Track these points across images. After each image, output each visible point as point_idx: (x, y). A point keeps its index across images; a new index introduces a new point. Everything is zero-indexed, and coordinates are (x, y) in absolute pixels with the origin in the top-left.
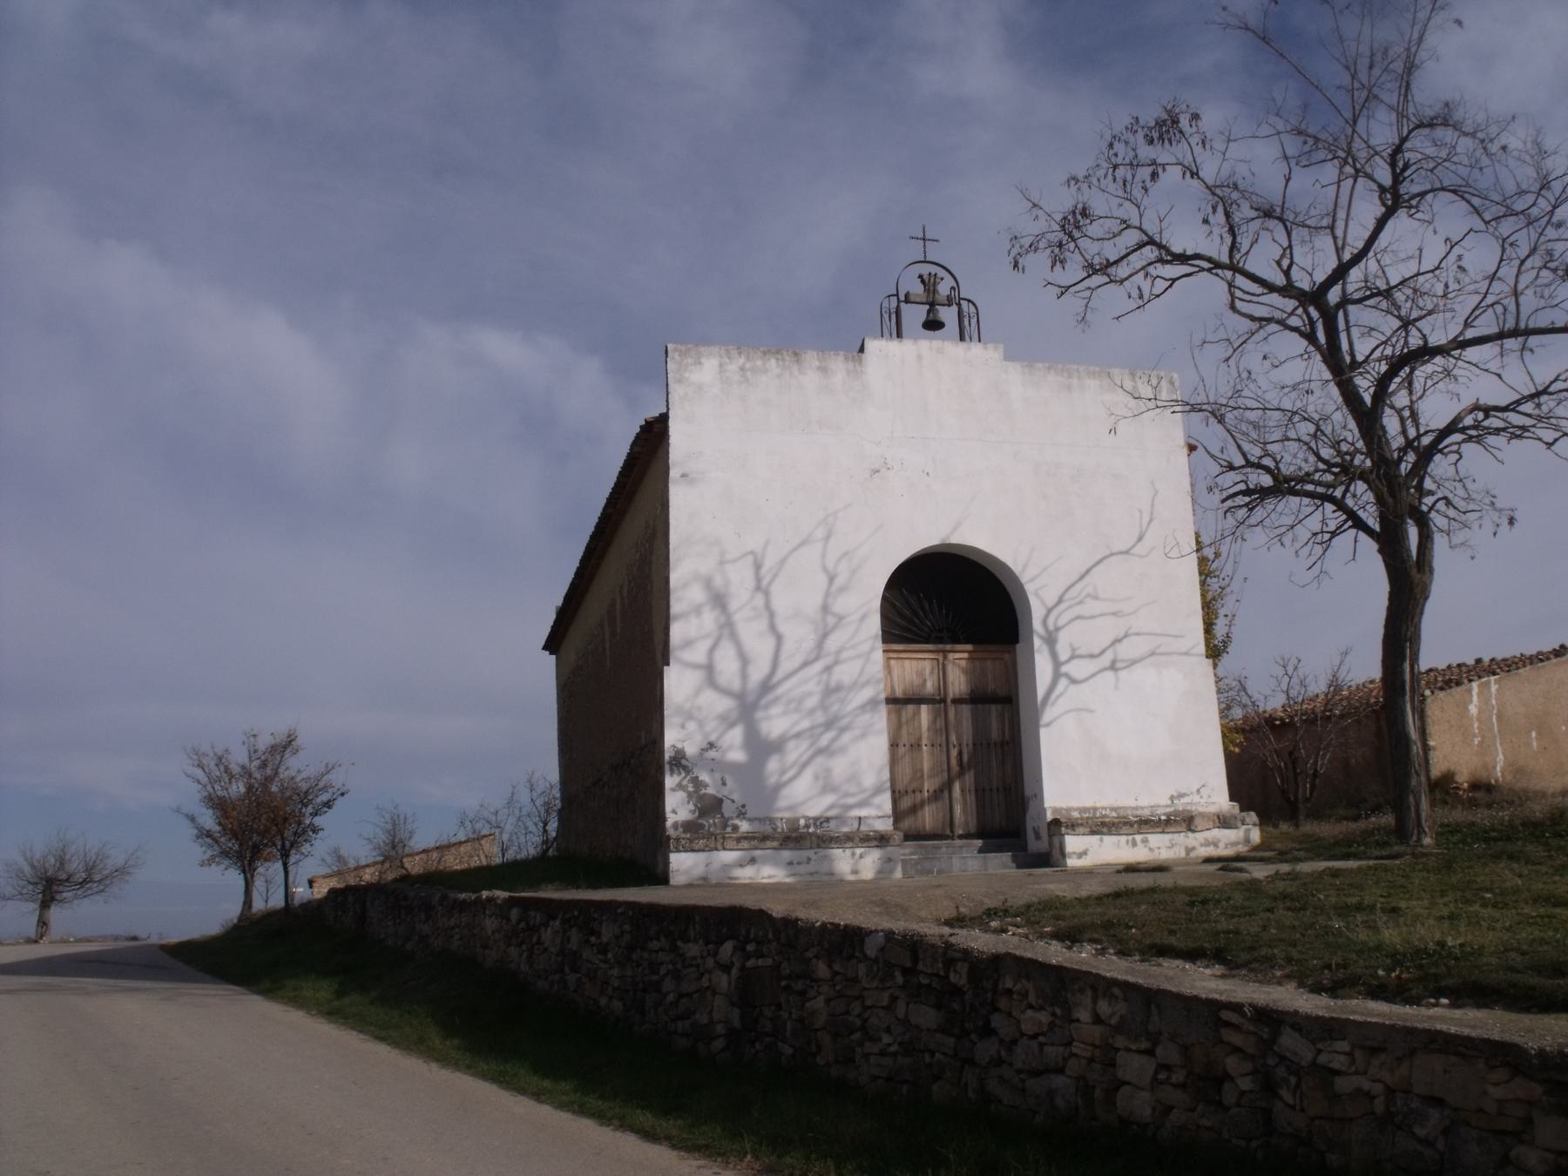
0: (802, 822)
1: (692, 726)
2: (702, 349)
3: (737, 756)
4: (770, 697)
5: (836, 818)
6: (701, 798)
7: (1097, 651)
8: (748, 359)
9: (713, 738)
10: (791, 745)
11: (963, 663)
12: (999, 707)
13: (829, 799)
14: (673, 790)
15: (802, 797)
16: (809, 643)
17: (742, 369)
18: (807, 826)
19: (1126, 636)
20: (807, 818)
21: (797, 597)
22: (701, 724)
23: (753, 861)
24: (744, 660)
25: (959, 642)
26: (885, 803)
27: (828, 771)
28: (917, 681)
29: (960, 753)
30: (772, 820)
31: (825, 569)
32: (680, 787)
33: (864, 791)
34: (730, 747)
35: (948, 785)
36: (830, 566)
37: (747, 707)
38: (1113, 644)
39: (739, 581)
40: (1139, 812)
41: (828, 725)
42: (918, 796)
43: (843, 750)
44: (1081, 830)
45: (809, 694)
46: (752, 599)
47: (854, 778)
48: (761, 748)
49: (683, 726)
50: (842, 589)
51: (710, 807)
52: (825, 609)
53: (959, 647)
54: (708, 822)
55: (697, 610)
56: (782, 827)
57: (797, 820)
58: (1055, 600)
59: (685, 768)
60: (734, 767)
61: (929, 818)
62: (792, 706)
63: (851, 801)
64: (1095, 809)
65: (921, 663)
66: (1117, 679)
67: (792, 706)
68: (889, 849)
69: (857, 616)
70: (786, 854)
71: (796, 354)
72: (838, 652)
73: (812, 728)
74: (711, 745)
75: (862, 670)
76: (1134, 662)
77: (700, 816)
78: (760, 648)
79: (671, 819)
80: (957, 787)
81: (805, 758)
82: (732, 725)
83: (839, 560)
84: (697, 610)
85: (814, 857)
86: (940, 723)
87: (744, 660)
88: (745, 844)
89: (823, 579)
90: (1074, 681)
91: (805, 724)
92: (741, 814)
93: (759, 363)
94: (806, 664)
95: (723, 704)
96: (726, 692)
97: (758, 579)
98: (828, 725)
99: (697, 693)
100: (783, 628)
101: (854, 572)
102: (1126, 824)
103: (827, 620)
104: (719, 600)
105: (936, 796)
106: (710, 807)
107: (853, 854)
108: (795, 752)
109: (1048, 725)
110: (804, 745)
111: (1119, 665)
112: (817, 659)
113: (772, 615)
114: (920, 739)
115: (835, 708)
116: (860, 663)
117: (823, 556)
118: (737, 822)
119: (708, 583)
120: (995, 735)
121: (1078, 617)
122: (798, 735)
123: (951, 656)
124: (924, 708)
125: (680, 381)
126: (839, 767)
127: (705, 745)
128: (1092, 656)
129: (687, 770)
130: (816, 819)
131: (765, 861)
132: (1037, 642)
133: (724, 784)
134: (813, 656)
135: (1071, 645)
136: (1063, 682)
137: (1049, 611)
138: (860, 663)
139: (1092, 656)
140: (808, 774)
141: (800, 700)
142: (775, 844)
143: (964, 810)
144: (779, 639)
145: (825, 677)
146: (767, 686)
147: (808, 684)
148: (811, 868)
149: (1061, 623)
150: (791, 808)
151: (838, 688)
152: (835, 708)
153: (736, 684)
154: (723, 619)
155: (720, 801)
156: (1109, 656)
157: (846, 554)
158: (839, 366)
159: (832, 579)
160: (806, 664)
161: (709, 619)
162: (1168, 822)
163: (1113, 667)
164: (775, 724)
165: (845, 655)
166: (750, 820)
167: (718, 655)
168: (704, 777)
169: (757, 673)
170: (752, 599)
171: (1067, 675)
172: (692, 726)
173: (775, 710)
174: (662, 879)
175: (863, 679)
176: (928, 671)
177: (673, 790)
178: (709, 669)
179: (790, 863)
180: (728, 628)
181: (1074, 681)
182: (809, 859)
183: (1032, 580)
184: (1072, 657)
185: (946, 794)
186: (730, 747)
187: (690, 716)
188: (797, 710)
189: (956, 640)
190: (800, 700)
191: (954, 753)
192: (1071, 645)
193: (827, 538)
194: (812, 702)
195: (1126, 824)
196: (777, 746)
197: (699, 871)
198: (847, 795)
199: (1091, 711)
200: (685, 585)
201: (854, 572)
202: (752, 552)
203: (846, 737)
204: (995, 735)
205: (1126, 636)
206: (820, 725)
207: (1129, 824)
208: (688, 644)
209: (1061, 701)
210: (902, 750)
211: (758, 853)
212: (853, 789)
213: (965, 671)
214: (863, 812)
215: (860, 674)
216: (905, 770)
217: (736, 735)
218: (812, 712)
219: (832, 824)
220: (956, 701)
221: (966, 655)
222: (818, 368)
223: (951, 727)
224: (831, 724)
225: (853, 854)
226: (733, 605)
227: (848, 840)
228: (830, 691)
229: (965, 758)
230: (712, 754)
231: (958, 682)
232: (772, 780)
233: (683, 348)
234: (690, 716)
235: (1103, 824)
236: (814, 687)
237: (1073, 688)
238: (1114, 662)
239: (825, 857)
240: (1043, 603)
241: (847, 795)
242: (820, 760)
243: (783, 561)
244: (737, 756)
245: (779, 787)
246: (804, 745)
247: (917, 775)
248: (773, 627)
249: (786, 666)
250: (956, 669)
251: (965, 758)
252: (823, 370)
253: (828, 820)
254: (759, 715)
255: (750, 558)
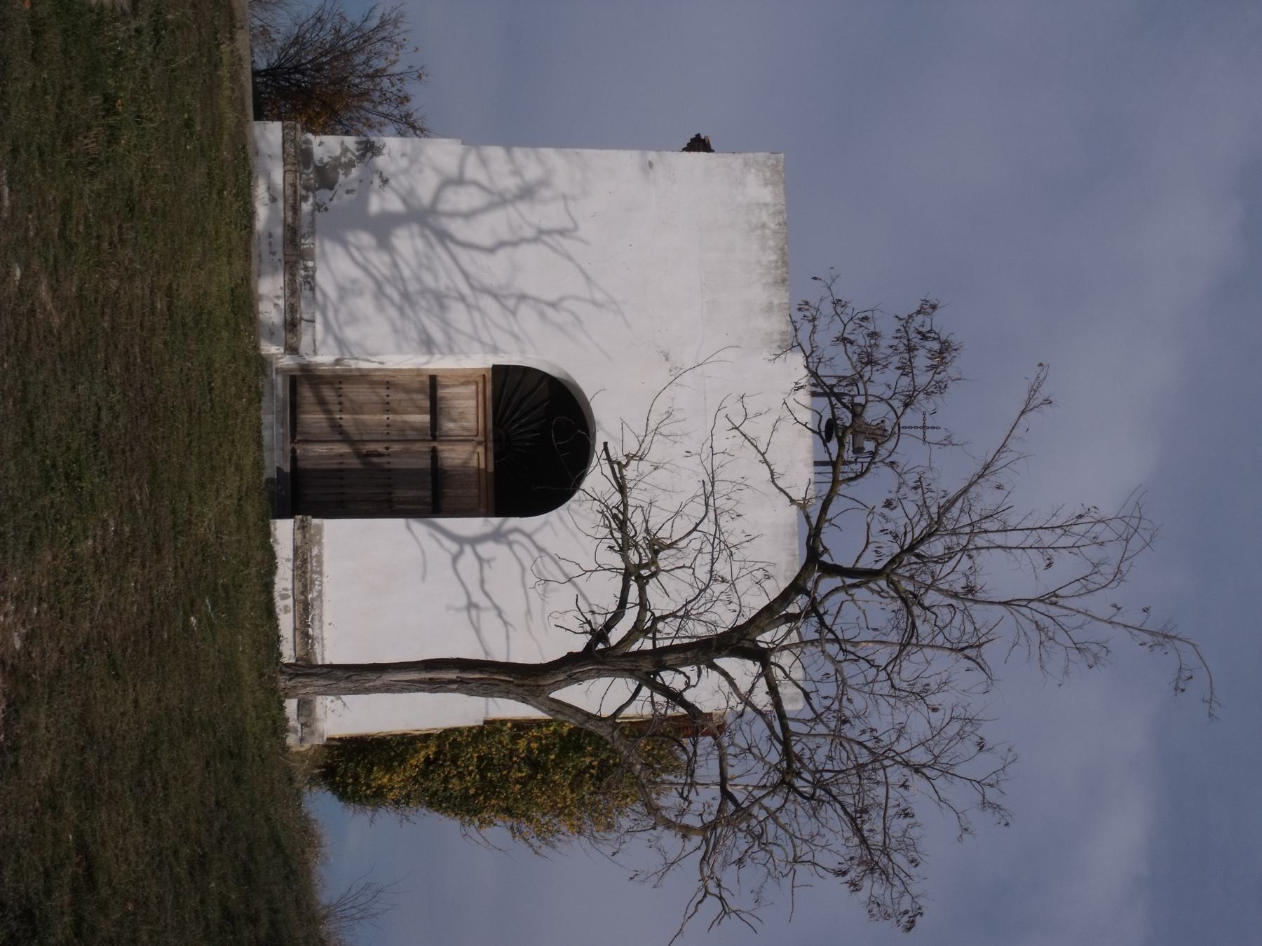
0: (310, 264)
1: (404, 163)
2: (781, 187)
3: (374, 205)
4: (434, 241)
5: (314, 298)
6: (335, 169)
7: (488, 587)
8: (775, 232)
9: (392, 182)
10: (386, 258)
11: (474, 463)
12: (429, 500)
13: (332, 293)
14: (342, 143)
15: (334, 266)
16: (487, 280)
17: (764, 226)
18: (306, 268)
19: (505, 623)
20: (314, 269)
21: (536, 270)
22: (405, 171)
23: (273, 200)
24: (469, 215)
25: (496, 457)
26: (324, 358)
27: (360, 293)
28: (454, 413)
29: (380, 455)
30: (312, 234)
31: (562, 299)
32: (345, 150)
33: (340, 328)
34: (383, 199)
35: (346, 439)
36: (566, 304)
37: (422, 216)
38: (496, 607)
39: (547, 214)
40: (316, 623)
41: (405, 295)
42: (337, 408)
43: (381, 309)
44: (299, 536)
45: (436, 277)
46: (530, 225)
47: (353, 319)
48: (383, 228)
49: (403, 155)
50: (542, 315)
51: (326, 177)
52: (523, 297)
53: (491, 457)
54: (310, 174)
55: (517, 172)
56: (306, 243)
57: (313, 259)
58: (541, 543)
59: (364, 155)
60: (364, 202)
61: (313, 418)
62: (424, 261)
63: (331, 314)
64: (321, 573)
65: (472, 417)
66: (458, 610)
67: (424, 261)
68: (283, 333)
69: (516, 330)
70: (279, 231)
71: (784, 281)
72: (479, 309)
73: (402, 279)
74: (385, 182)
75: (463, 333)
76: (477, 631)
77: (317, 168)
78: (482, 230)
79: (315, 140)
80: (344, 449)
81: (374, 271)
82: (405, 201)
83: (573, 314)
84: (517, 172)
85: (277, 258)
86: (411, 434)
87: (469, 215)
88: (289, 192)
89: (552, 296)
90: (455, 559)
91: (407, 273)
92: (318, 207)
93: (771, 243)
94: (466, 275)
95: (425, 193)
96: (437, 197)
97: (550, 232)
98: (405, 295)
99: (437, 170)
100: (502, 254)
101: (561, 328)
102: (305, 586)
103: (511, 299)
104: (527, 193)
105: (336, 427)
106: (326, 177)
107: (278, 297)
108: (379, 262)
109: (408, 527)
110: (386, 271)
111: (474, 612)
112: (472, 286)
113: (514, 244)
114: (395, 412)
115: (423, 303)
116: (469, 330)
117: (577, 298)
118: (311, 200)
119: (544, 183)
120: (400, 493)
121: (523, 568)
122: (395, 265)
123: (481, 449)
124: (427, 418)
125: (746, 164)
126: (365, 304)
127: (385, 175)
128: (482, 582)
129: (362, 157)
130: (313, 277)
131: (273, 211)
132: (496, 521)
133: (348, 192)
134: (474, 283)
135: (494, 559)
136: (454, 547)
137: (529, 536)
138: (469, 330)
139: (482, 582)
140: (356, 273)
141: (430, 269)
142: (290, 220)
143: (321, 457)
144: (491, 250)
145: (454, 294)
146: (444, 237)
147: (445, 277)
148: (266, 256)
149: (516, 547)
150: (324, 254)
151: (443, 307)
152: (423, 303)
153: (444, 206)
154: (508, 196)
155: (331, 187)
156: (478, 597)
157: (579, 321)
158: (777, 324)
159: (553, 305)
160: (466, 275)
161: (509, 183)
162: (306, 636)
163: (471, 605)
164: (406, 242)
165: (476, 315)
166: (312, 213)
167: (473, 190)
168: (355, 172)
169: (457, 228)
170: (530, 225)
171: (461, 552)
172: (404, 163)
173: (420, 243)
174: (259, 116)
175: (452, 332)
176: (466, 424)
177: (342, 143)
178: (459, 181)
179: (270, 236)
180: (500, 201)
181: (455, 559)
182: (274, 254)
183: (561, 518)
184: (480, 559)
185: (337, 437)
186: (383, 199)
187: (413, 161)
188: (420, 265)
189: (497, 456)
190: (430, 269)
191: (380, 448)
192: (494, 559)
193: (595, 303)
194: (428, 279)
195: (305, 586)
196: (384, 243)
197: (263, 146)
198: (336, 311)
199: (423, 578)
200: (541, 161)
201: (561, 328)
202: (576, 228)
203: (393, 313)
204: (400, 493)
205: (505, 623)
206: (405, 288)
207: (305, 590)
208: (484, 162)
209: (435, 544)
210: (383, 392)
211: (281, 204)
212: (342, 317)
213: (465, 464)
214: (319, 326)
215: (457, 330)
216: (358, 393)
217: (395, 205)
218: (419, 279)
219: (307, 293)
220: (434, 452)
221: (482, 466)
222: (771, 303)
223: (408, 446)
224: (404, 297)
225: (278, 297)
226: (523, 207)
227: (292, 291)
228: (440, 300)
229: (376, 460)
230: (377, 181)
231: (456, 455)
232: (351, 237)
233: (780, 168)
234: (413, 161)
235: (305, 561)
236: (443, 282)
237: (447, 559)
238: (477, 607)
239: (277, 270)
240: (537, 530)
241: (336, 311)
242: (370, 285)
243: (570, 258)
244: (374, 205)
245: (345, 244)
246: (386, 271)
247: (357, 409)
248: (502, 244)
249: (464, 256)
250: (465, 454)
251: (376, 460)
252: (770, 308)
253: (312, 289)
254: (415, 228)
255: (570, 225)
